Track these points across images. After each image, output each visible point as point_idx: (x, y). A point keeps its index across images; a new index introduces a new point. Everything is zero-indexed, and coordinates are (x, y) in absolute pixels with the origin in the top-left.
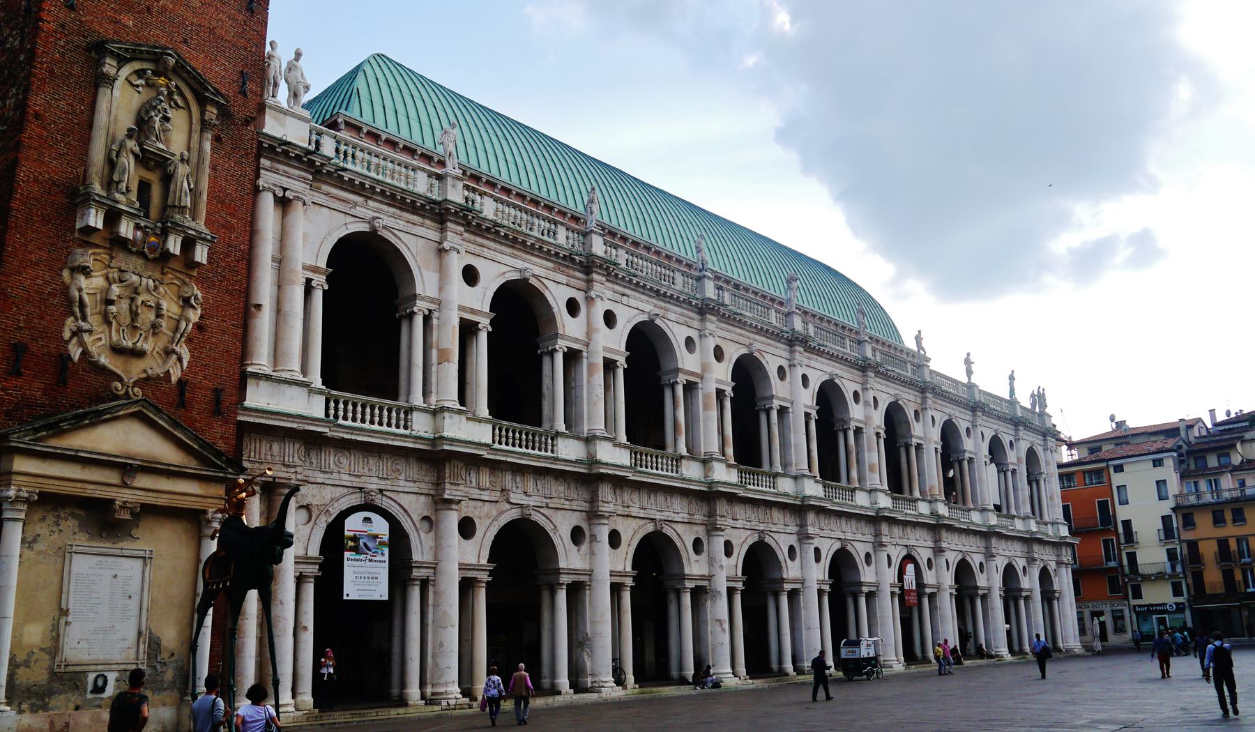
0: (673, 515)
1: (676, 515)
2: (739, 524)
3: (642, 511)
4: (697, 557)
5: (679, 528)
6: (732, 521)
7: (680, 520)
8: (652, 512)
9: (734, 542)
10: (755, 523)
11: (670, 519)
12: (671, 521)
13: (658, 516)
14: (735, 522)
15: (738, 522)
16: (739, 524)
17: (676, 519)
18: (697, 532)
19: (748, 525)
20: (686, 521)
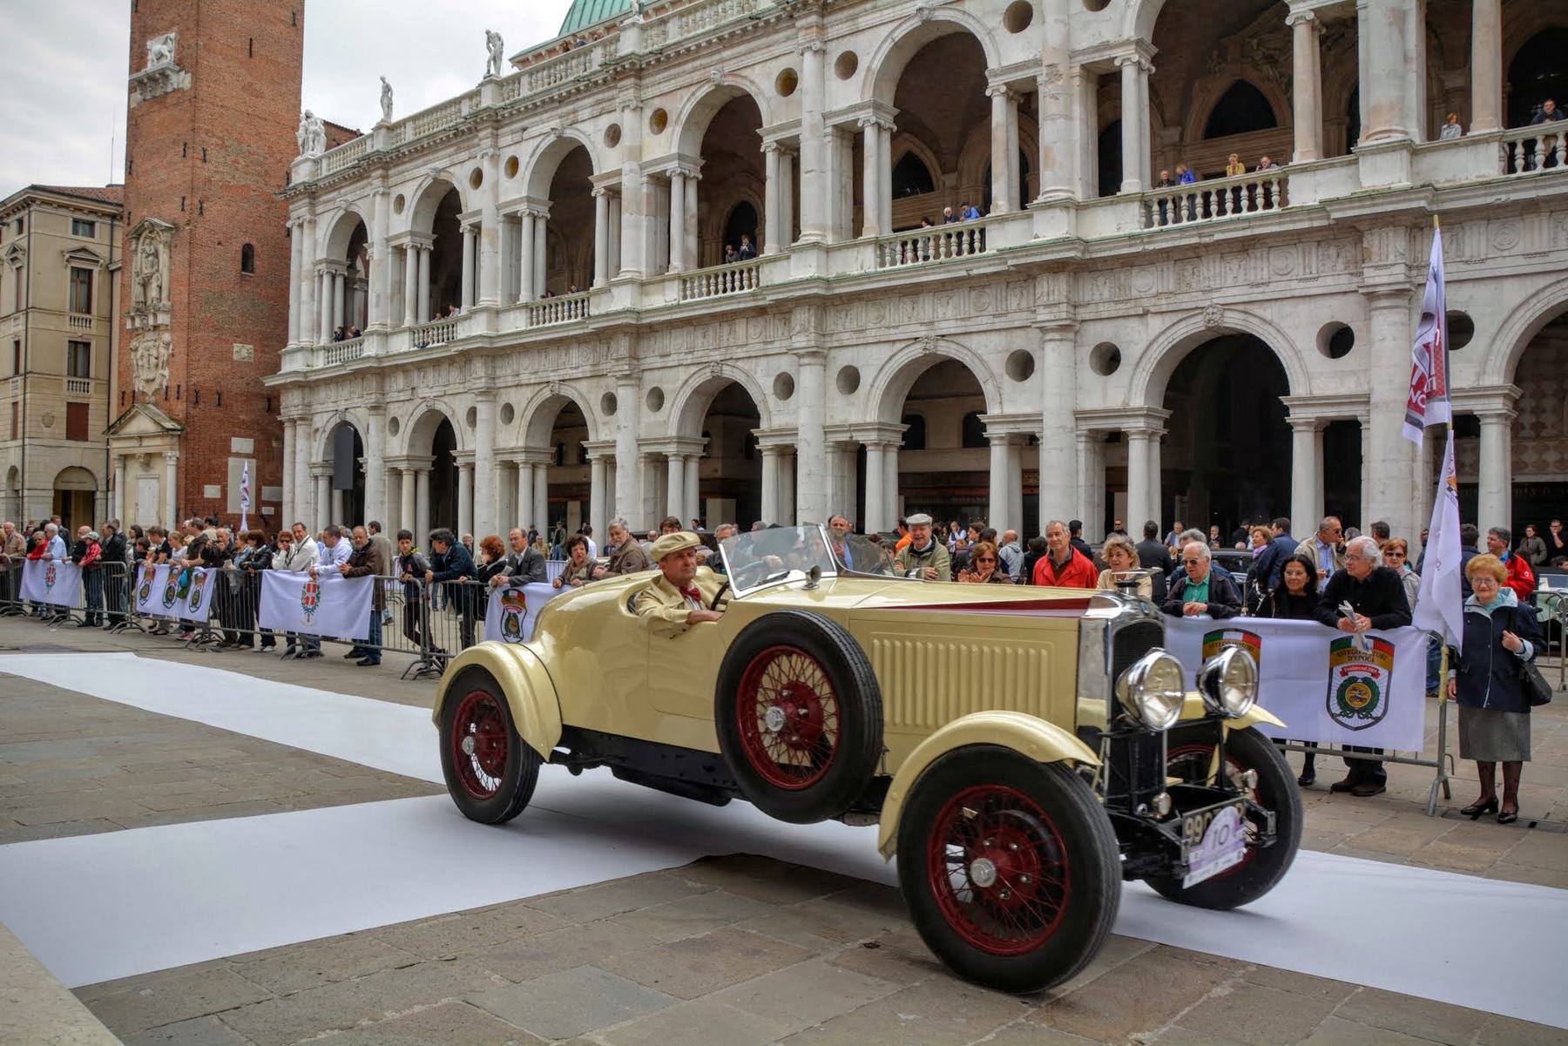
0: (571, 372)
1: (575, 371)
2: (671, 361)
3: (533, 376)
4: (608, 418)
5: (583, 386)
6: (659, 359)
7: (580, 375)
8: (545, 374)
9: (665, 388)
10: (701, 353)
11: (567, 377)
12: (569, 380)
13: (553, 377)
14: (665, 359)
15: (670, 358)
16: (671, 361)
17: (574, 376)
18: (607, 387)
19: (689, 359)
20: (588, 375)
